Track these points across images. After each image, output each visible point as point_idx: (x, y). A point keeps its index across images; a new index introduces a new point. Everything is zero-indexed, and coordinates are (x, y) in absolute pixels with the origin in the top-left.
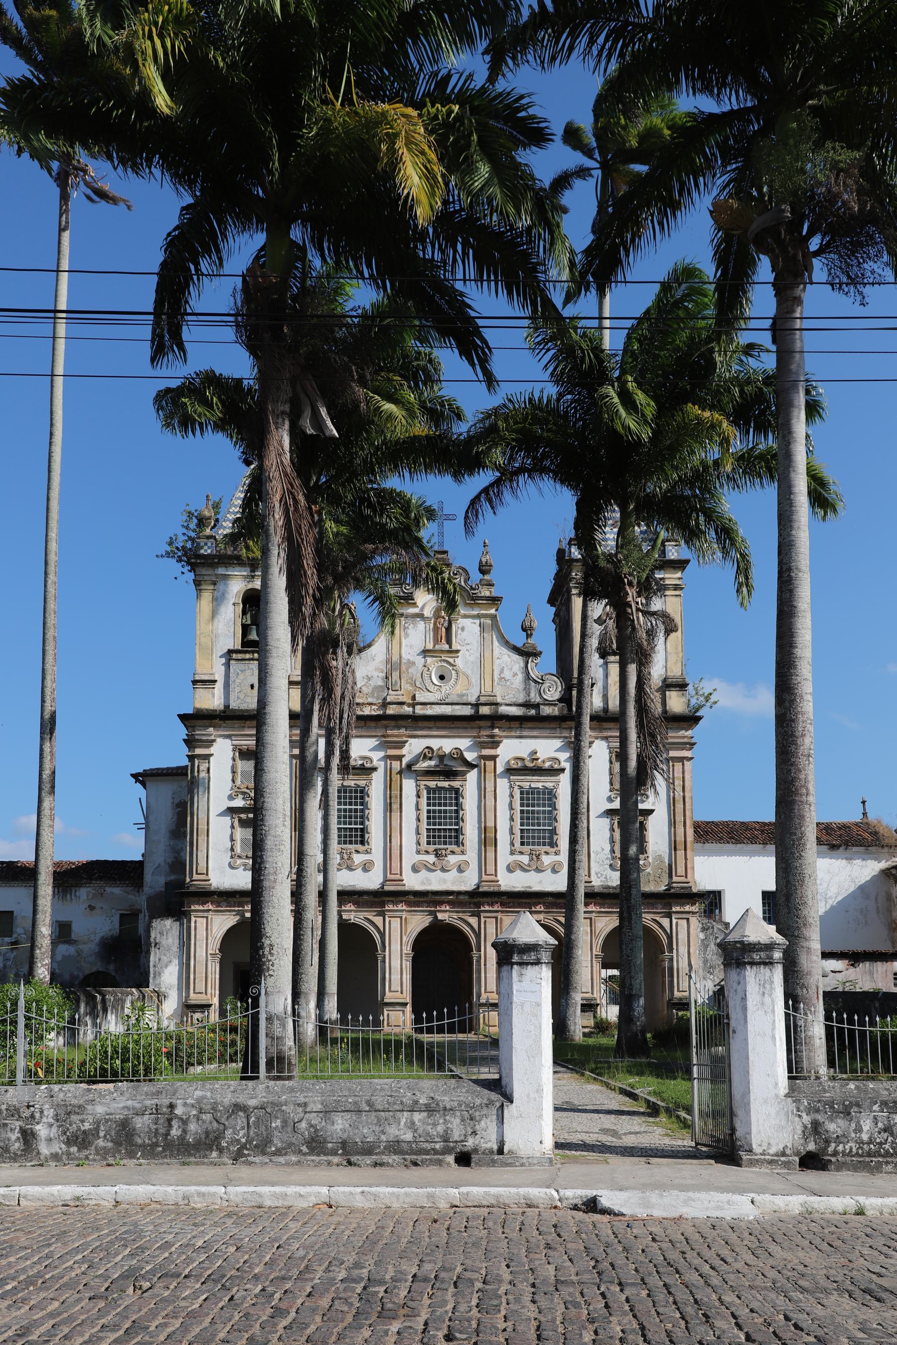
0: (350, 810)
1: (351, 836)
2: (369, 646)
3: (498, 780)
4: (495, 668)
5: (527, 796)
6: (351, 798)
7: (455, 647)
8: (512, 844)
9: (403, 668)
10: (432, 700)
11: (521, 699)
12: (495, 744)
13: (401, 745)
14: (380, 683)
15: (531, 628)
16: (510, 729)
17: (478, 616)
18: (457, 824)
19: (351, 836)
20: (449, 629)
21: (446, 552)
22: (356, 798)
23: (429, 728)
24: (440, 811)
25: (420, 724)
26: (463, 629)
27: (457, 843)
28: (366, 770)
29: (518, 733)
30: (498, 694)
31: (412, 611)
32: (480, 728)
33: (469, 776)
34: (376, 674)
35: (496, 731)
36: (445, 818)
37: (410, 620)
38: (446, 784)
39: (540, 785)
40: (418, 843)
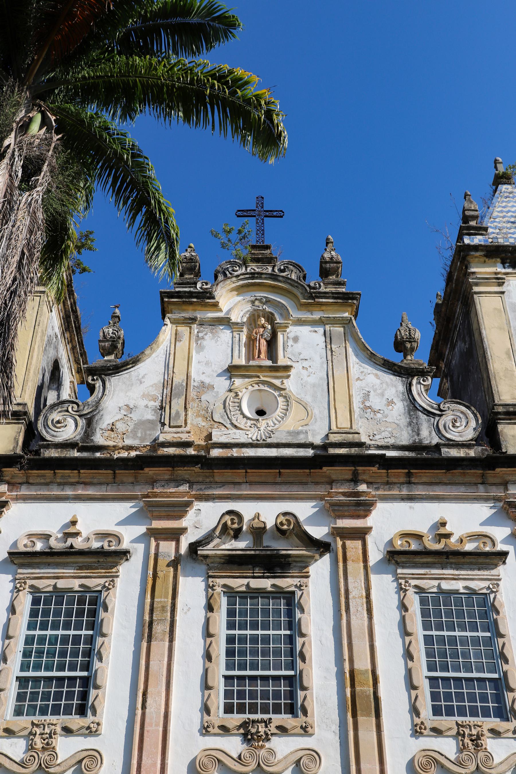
0: (65, 639)
1: (58, 696)
2: (135, 361)
3: (373, 578)
4: (354, 392)
5: (438, 608)
6: (69, 614)
7: (282, 361)
8: (415, 711)
9: (192, 394)
10: (243, 439)
11: (405, 438)
12: (363, 508)
13: (180, 509)
14: (150, 416)
15: (411, 339)
16: (389, 484)
17: (321, 322)
18: (292, 666)
19: (58, 696)
20: (272, 343)
21: (267, 247)
22: (80, 613)
23: (235, 484)
24: (254, 639)
25: (219, 475)
26: (296, 339)
27: (291, 709)
28: (107, 557)
29: (405, 492)
30: (361, 431)
31: (212, 315)
32: (331, 482)
33: (312, 569)
34: (142, 403)
35: (363, 487)
36: (266, 653)
37: (207, 329)
38: (266, 584)
39: (459, 586)
40: (206, 709)
